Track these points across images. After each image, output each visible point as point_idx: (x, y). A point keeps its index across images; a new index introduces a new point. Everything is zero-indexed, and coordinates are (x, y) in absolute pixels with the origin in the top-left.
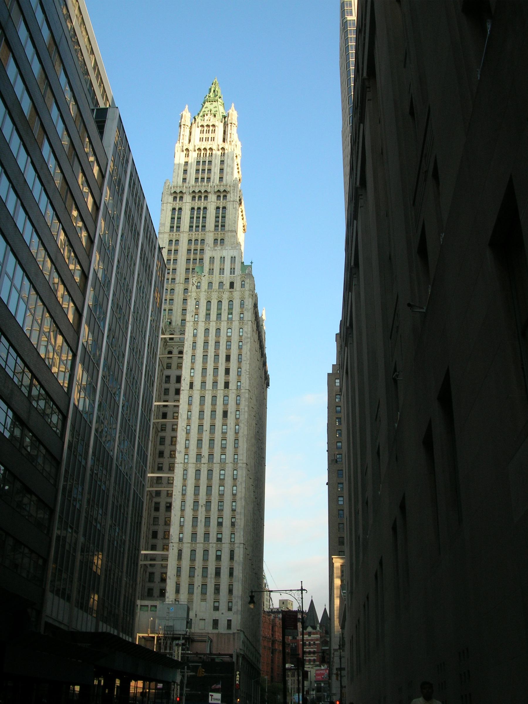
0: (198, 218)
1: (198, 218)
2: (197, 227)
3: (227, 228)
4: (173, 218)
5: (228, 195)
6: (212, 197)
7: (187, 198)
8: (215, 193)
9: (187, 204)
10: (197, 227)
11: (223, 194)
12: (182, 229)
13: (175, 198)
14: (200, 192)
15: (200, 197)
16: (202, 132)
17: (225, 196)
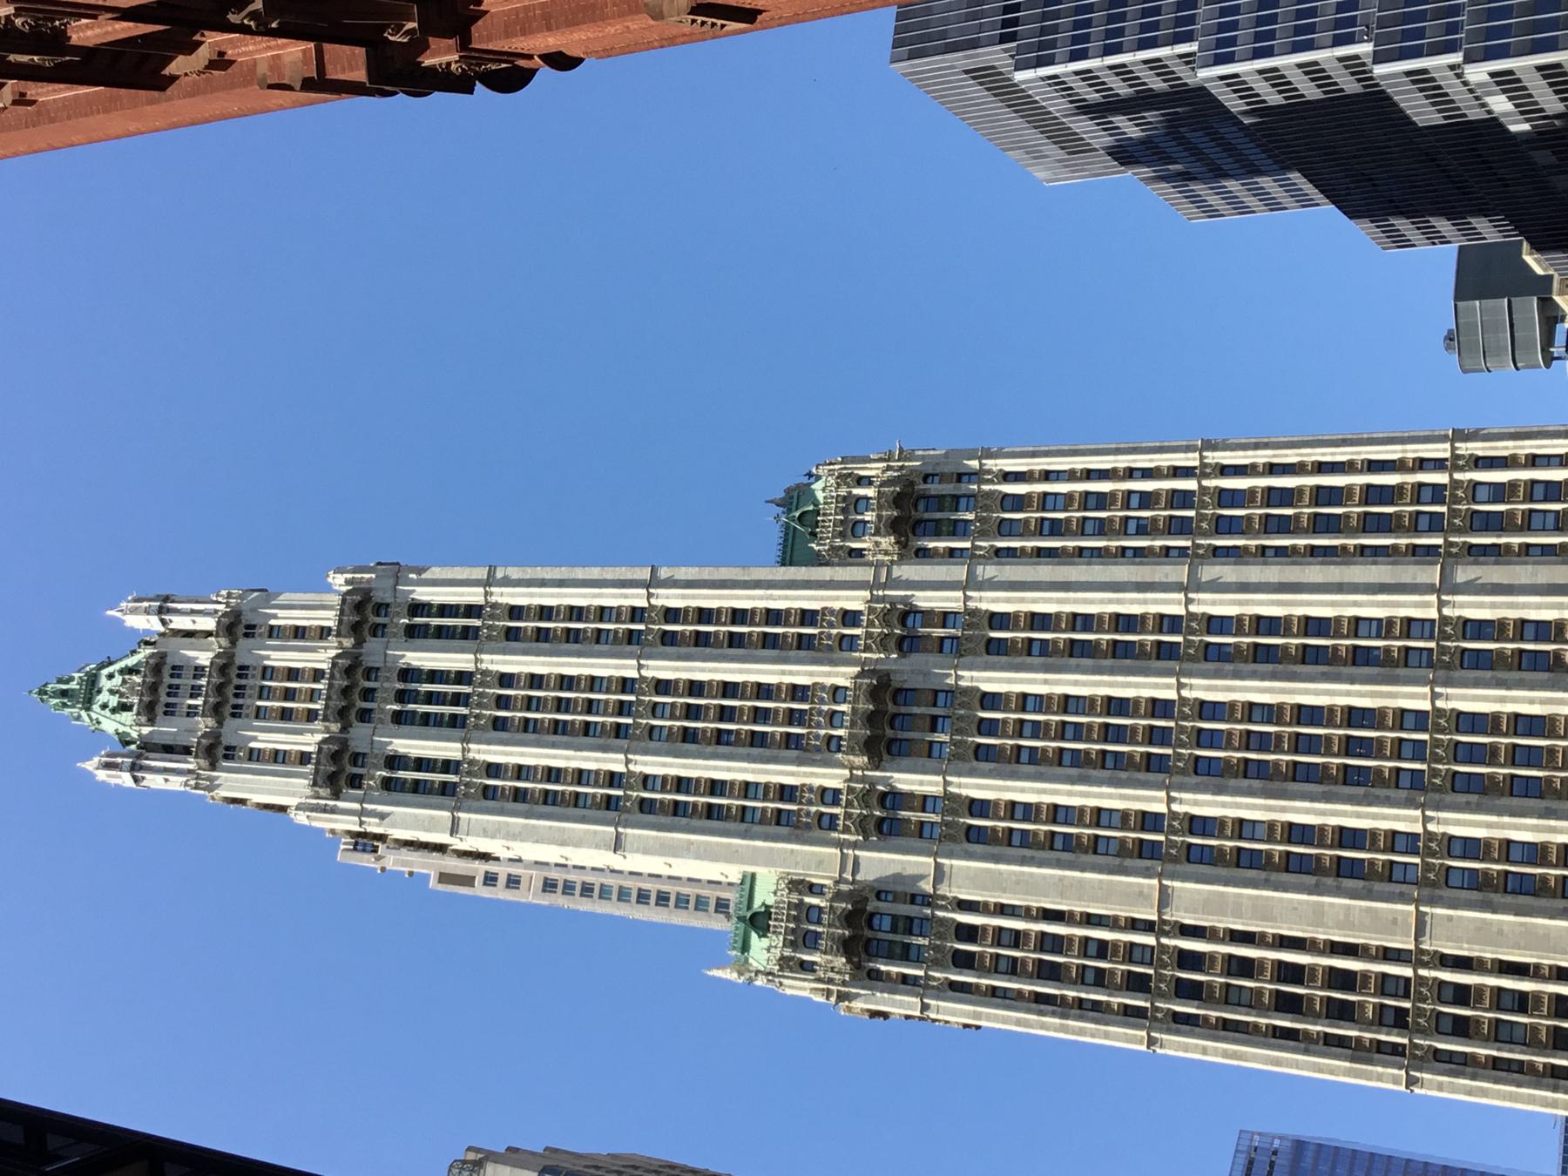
2: (457, 699)
5: (380, 596)
7: (360, 735)
10: (457, 699)
13: (355, 782)
14: (346, 692)
15: (368, 694)
16: (170, 710)
17: (382, 608)
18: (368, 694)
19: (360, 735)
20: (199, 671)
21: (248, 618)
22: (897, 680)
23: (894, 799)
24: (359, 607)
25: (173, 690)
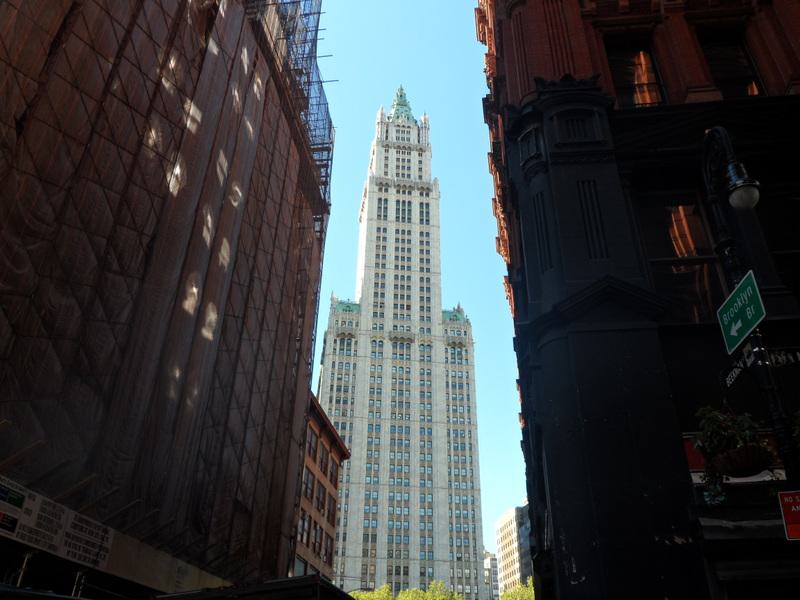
0: (404, 210)
1: (404, 210)
2: (404, 218)
3: (431, 222)
4: (379, 208)
5: (431, 194)
6: (416, 193)
7: (392, 191)
8: (418, 189)
9: (392, 196)
10: (404, 218)
11: (426, 191)
12: (389, 219)
13: (380, 190)
15: (404, 192)
16: (398, 131)
17: (427, 195)
18: (404, 192)
19: (392, 191)
20: (409, 140)
21: (424, 154)
22: (412, 344)
23: (381, 344)
24: (428, 189)
25: (403, 132)
